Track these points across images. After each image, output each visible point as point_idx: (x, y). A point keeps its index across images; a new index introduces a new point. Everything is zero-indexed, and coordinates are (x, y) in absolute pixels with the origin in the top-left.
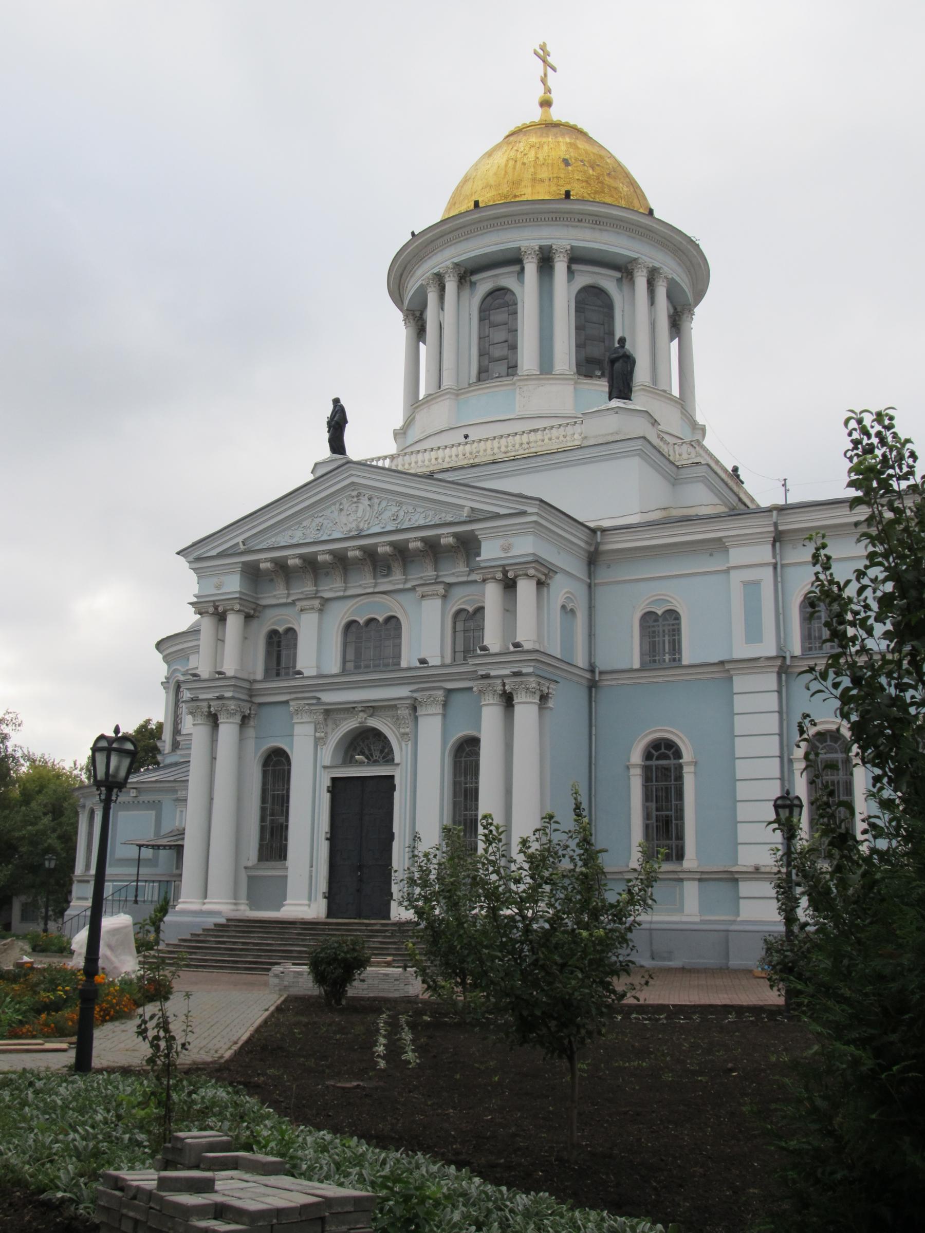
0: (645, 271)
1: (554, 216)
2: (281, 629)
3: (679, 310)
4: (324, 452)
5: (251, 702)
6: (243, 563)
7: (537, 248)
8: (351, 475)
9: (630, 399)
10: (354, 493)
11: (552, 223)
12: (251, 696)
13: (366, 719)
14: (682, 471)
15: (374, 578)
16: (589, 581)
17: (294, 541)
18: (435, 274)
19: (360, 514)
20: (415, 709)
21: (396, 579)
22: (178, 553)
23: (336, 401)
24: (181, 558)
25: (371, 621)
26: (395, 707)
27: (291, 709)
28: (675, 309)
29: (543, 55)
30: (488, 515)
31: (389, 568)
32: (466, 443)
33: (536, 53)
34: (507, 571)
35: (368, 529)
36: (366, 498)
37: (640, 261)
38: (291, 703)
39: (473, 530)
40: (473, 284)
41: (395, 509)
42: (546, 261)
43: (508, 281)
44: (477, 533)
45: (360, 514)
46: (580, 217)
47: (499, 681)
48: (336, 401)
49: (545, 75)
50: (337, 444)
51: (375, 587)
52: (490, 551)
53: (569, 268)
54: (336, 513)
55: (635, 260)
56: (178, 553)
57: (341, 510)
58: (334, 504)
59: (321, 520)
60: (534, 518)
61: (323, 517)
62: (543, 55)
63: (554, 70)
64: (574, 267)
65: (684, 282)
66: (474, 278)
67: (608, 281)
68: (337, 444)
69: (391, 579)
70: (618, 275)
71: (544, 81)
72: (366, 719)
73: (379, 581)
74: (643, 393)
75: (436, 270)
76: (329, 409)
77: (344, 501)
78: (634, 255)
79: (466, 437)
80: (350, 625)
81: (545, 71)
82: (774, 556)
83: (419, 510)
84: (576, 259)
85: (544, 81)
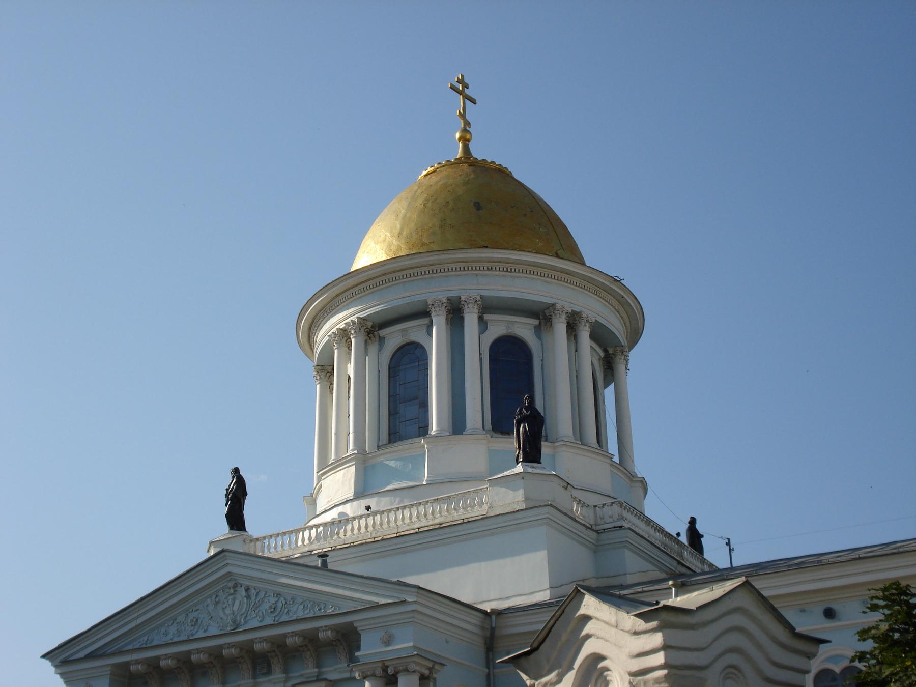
0: (564, 316)
1: (460, 265)
3: (611, 351)
4: (222, 529)
6: (114, 665)
7: (445, 300)
8: (227, 565)
9: (539, 462)
10: (231, 584)
14: (604, 536)
15: (255, 677)
16: (487, 670)
17: (168, 639)
18: (341, 329)
19: (236, 608)
22: (44, 656)
24: (47, 663)
28: (605, 351)
29: (461, 88)
31: (269, 665)
32: (368, 515)
33: (453, 88)
35: (246, 622)
37: (558, 306)
39: (351, 623)
41: (273, 600)
42: (455, 313)
44: (356, 625)
45: (236, 608)
46: (489, 265)
50: (236, 519)
53: (481, 318)
54: (211, 607)
55: (553, 305)
56: (44, 656)
57: (217, 603)
58: (210, 597)
59: (195, 614)
60: (414, 607)
61: (199, 611)
62: (461, 88)
63: (474, 101)
64: (487, 317)
65: (616, 325)
66: (383, 333)
67: (523, 329)
68: (236, 519)
69: (271, 677)
70: (536, 322)
71: (463, 116)
73: (258, 680)
74: (564, 449)
76: (227, 481)
79: (368, 508)
84: (488, 307)
85: (463, 116)
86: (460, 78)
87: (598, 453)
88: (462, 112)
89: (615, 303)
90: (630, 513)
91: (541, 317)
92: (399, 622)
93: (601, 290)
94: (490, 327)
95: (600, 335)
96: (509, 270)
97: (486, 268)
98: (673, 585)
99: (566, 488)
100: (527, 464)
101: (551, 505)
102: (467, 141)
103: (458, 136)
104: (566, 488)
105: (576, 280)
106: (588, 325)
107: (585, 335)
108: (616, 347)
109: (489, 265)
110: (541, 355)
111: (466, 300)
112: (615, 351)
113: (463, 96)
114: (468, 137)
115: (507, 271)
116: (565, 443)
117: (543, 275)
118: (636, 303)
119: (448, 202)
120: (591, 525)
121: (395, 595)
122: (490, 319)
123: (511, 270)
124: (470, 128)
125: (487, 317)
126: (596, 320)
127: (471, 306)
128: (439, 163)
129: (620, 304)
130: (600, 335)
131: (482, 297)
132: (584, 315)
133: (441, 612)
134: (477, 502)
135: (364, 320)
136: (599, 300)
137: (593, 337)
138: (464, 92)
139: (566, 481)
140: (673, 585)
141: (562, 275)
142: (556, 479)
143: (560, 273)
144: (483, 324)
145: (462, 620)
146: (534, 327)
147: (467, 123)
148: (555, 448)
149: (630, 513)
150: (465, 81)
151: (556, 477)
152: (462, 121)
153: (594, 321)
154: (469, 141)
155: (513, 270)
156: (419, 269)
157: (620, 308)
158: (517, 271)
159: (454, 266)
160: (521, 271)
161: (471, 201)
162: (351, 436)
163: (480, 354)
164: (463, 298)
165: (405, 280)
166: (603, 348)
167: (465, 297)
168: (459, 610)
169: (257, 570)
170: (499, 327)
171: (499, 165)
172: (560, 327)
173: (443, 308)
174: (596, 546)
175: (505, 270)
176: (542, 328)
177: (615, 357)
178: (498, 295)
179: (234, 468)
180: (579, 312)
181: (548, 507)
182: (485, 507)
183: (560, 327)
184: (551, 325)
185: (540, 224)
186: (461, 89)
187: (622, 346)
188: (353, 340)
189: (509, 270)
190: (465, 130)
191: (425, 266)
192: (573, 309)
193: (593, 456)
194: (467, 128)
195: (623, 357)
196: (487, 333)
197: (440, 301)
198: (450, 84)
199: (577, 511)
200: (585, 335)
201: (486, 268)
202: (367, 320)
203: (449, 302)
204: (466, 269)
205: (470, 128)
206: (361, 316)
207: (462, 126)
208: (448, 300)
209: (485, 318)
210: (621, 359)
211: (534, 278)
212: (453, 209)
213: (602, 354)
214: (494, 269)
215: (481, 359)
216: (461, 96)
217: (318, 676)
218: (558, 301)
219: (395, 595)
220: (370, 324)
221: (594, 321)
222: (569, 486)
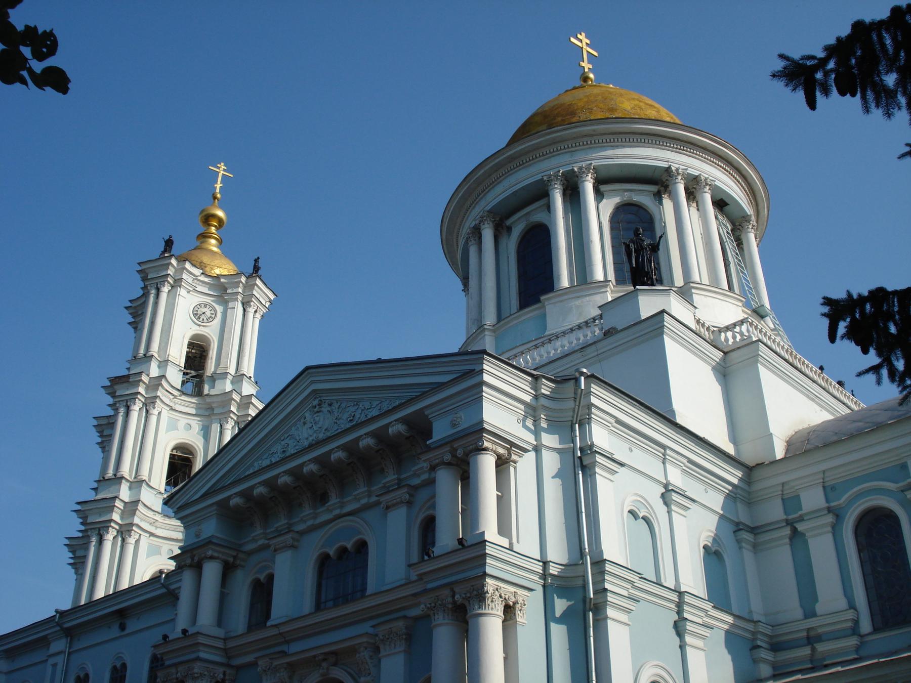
2: (262, 577)
5: (228, 665)
6: (217, 503)
10: (316, 402)
12: (229, 658)
13: (328, 669)
20: (377, 650)
21: (360, 494)
25: (343, 551)
26: (353, 650)
27: (259, 669)
30: (435, 386)
34: (456, 450)
36: (326, 405)
38: (260, 663)
40: (509, 229)
43: (539, 217)
47: (447, 592)
51: (342, 507)
52: (440, 431)
64: (603, 188)
67: (642, 196)
70: (654, 188)
72: (328, 669)
75: (472, 225)
77: (307, 415)
80: (324, 561)
83: (375, 403)
217: (398, 484)
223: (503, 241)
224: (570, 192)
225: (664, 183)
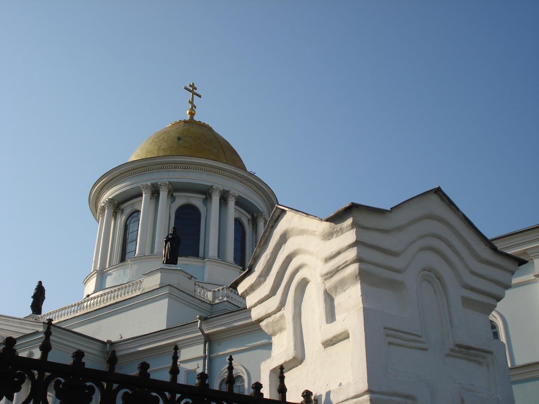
0: (218, 192)
1: (160, 166)
3: (255, 216)
11: (159, 170)
14: (214, 306)
23: (40, 283)
28: (253, 216)
29: (192, 89)
33: (186, 88)
37: (214, 187)
40: (122, 211)
48: (40, 283)
49: (192, 99)
55: (212, 187)
62: (192, 89)
63: (200, 96)
64: (175, 194)
66: (123, 206)
67: (196, 201)
70: (204, 197)
78: (210, 184)
81: (193, 96)
82: (205, 352)
85: (191, 102)
86: (192, 84)
87: (231, 265)
88: (191, 101)
89: (255, 188)
90: (233, 293)
91: (207, 194)
92: (63, 350)
93: (244, 180)
94: (177, 200)
95: (241, 203)
96: (186, 168)
97: (173, 167)
98: (200, 318)
99: (191, 279)
100: (167, 265)
101: (170, 285)
102: (192, 114)
103: (188, 112)
104: (191, 279)
105: (227, 174)
106: (233, 198)
107: (231, 203)
108: (258, 213)
109: (175, 165)
110: (206, 215)
111: (161, 184)
112: (258, 215)
113: (193, 93)
114: (193, 112)
115: (185, 168)
116: (209, 259)
117: (206, 170)
118: (269, 189)
119: (164, 138)
120: (210, 302)
121: (31, 328)
122: (176, 195)
123: (187, 168)
124: (195, 108)
125: (175, 194)
126: (239, 195)
127: (163, 187)
128: (171, 124)
129: (258, 188)
130: (241, 203)
131: (170, 183)
132: (231, 192)
133: (73, 342)
134: (138, 288)
135: (113, 200)
136: (243, 185)
137: (237, 203)
138: (193, 91)
139: (190, 275)
140: (200, 318)
141: (252, 186)
142: (181, 272)
143: (216, 169)
144: (171, 196)
145: (84, 346)
146: (203, 200)
147: (194, 106)
148: (204, 262)
149: (236, 295)
150: (194, 86)
151: (181, 271)
152: (191, 105)
153: (238, 196)
154: (194, 115)
155: (188, 168)
156: (138, 169)
157: (258, 191)
158: (191, 168)
159: (156, 167)
160: (193, 168)
161: (176, 136)
162: (99, 261)
163: (170, 214)
164: (159, 183)
165: (131, 176)
166: (251, 214)
167: (160, 183)
168: (86, 341)
169: (61, 338)
170: (181, 200)
171: (204, 123)
172: (216, 199)
173: (149, 190)
174: (211, 313)
175: (184, 168)
176: (208, 199)
177: (258, 218)
178: (179, 181)
179: (39, 282)
180: (228, 191)
181: (168, 286)
182: (141, 290)
183: (216, 199)
184: (227, 204)
185: (214, 148)
186: (192, 90)
187: (261, 212)
188: (106, 211)
189: (186, 168)
190: (192, 109)
191: (141, 168)
192: (224, 189)
193: (226, 267)
194: (194, 108)
195: (262, 218)
196: (173, 203)
197: (147, 186)
198: (184, 87)
199: (200, 293)
200: (231, 203)
201: (173, 167)
202: (114, 200)
203: (153, 186)
204: (162, 168)
205: (195, 108)
206: (110, 198)
207: (191, 107)
208: (152, 185)
209: (174, 195)
210: (261, 219)
211: (201, 172)
212: (166, 141)
213: (250, 217)
214: (177, 167)
215: (170, 217)
216: (191, 93)
218: (214, 184)
219: (31, 328)
220: (116, 202)
221: (238, 196)
222: (192, 278)
223: (119, 216)
224: (157, 195)
225: (210, 193)
